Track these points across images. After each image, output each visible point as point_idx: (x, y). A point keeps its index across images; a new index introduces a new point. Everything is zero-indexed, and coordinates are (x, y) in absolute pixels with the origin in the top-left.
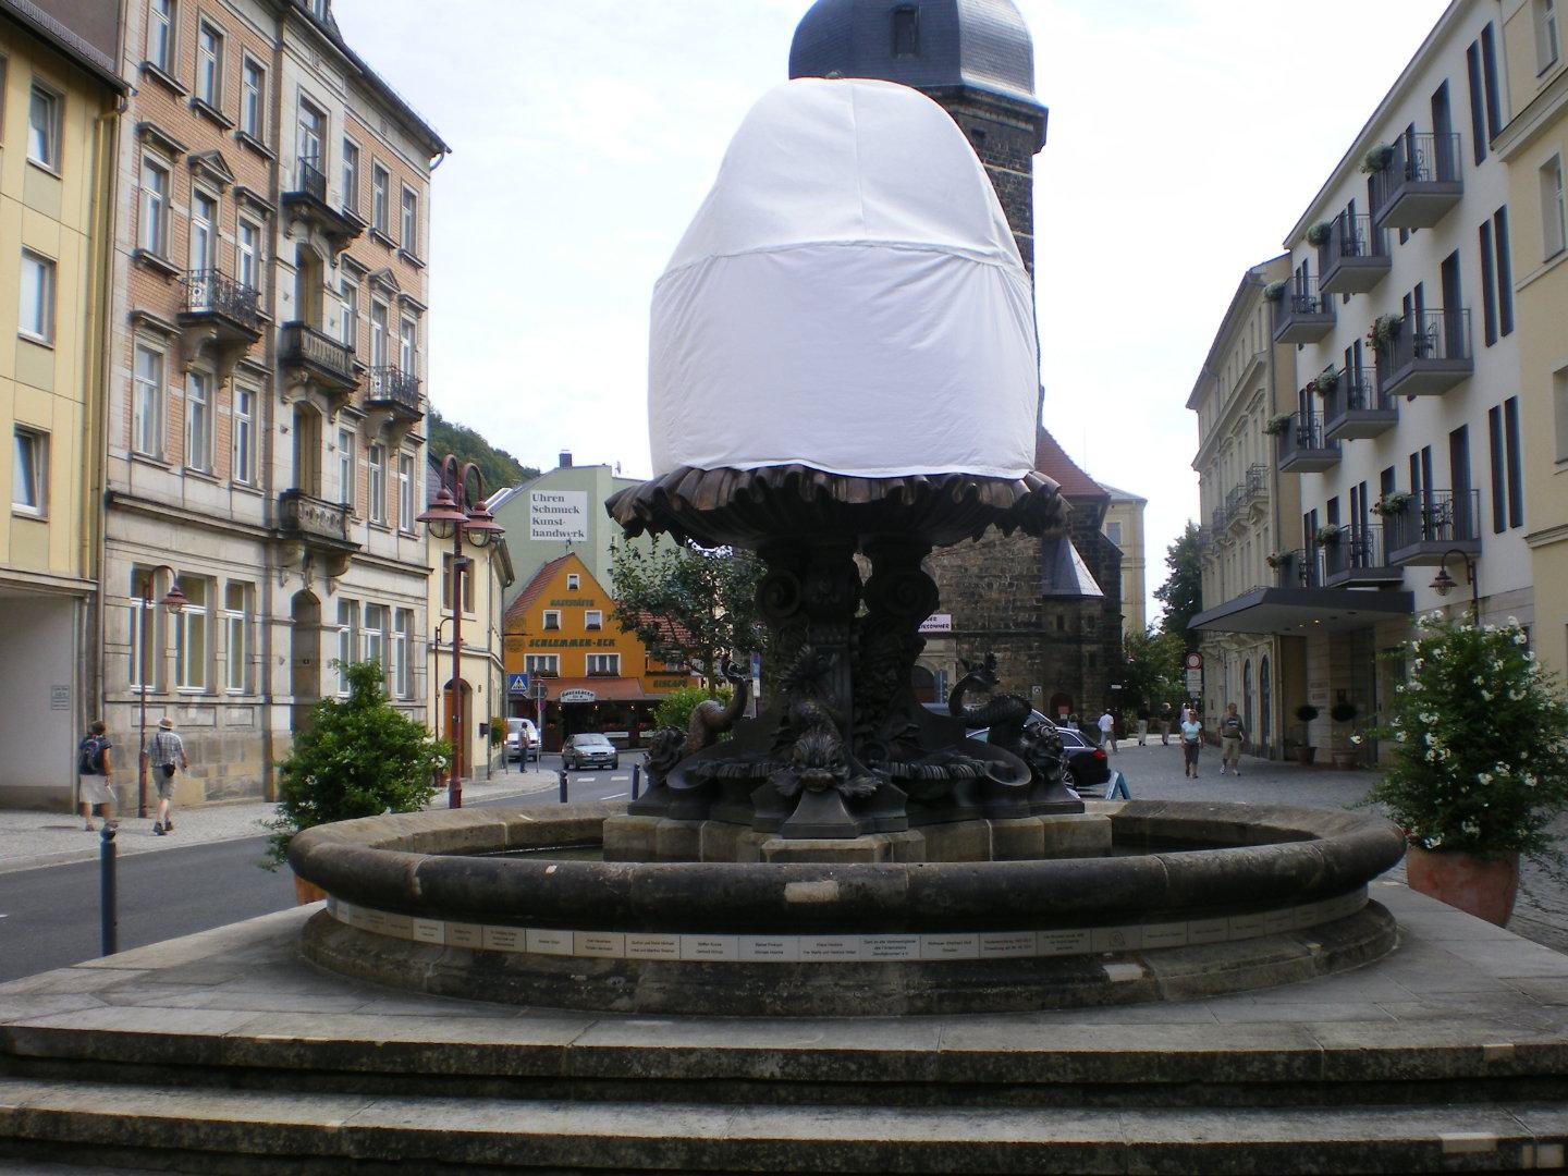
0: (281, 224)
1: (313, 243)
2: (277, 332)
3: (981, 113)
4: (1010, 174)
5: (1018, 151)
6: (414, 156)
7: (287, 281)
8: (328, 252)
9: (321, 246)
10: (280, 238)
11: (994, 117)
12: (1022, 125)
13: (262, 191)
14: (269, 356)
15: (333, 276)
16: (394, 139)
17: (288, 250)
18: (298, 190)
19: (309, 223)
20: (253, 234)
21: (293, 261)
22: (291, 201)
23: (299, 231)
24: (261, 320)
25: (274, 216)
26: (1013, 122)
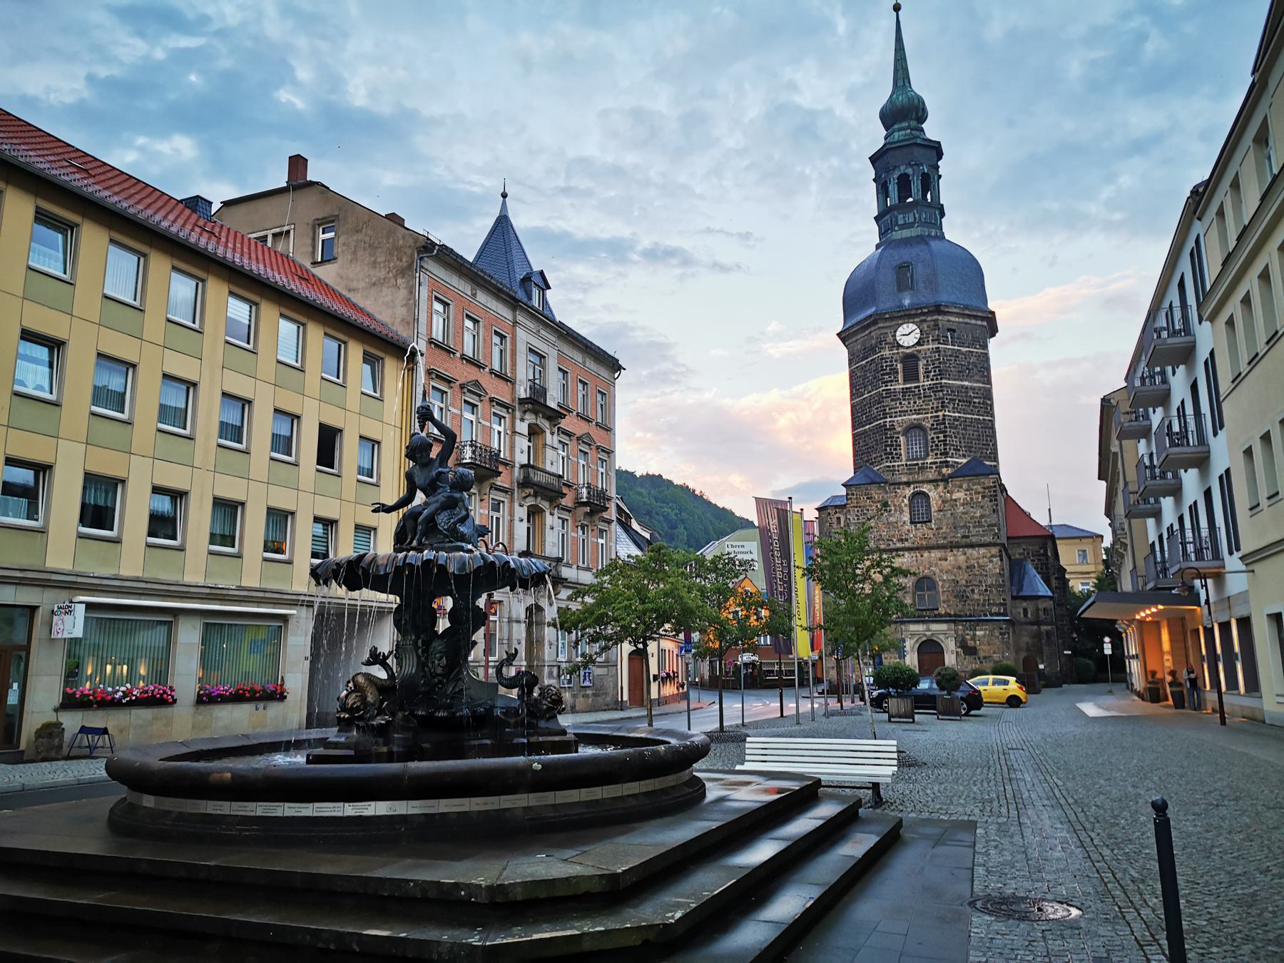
0: (518, 414)
1: (538, 422)
2: (517, 470)
3: (952, 319)
4: (972, 352)
5: (978, 338)
6: (604, 373)
7: (522, 443)
8: (548, 426)
9: (545, 424)
10: (518, 421)
11: (961, 320)
12: (979, 323)
13: (507, 400)
14: (512, 483)
15: (551, 439)
16: (591, 365)
17: (523, 427)
18: (528, 396)
19: (536, 413)
20: (503, 420)
21: (526, 433)
22: (522, 402)
23: (530, 418)
24: (506, 465)
25: (514, 410)
26: (973, 322)
